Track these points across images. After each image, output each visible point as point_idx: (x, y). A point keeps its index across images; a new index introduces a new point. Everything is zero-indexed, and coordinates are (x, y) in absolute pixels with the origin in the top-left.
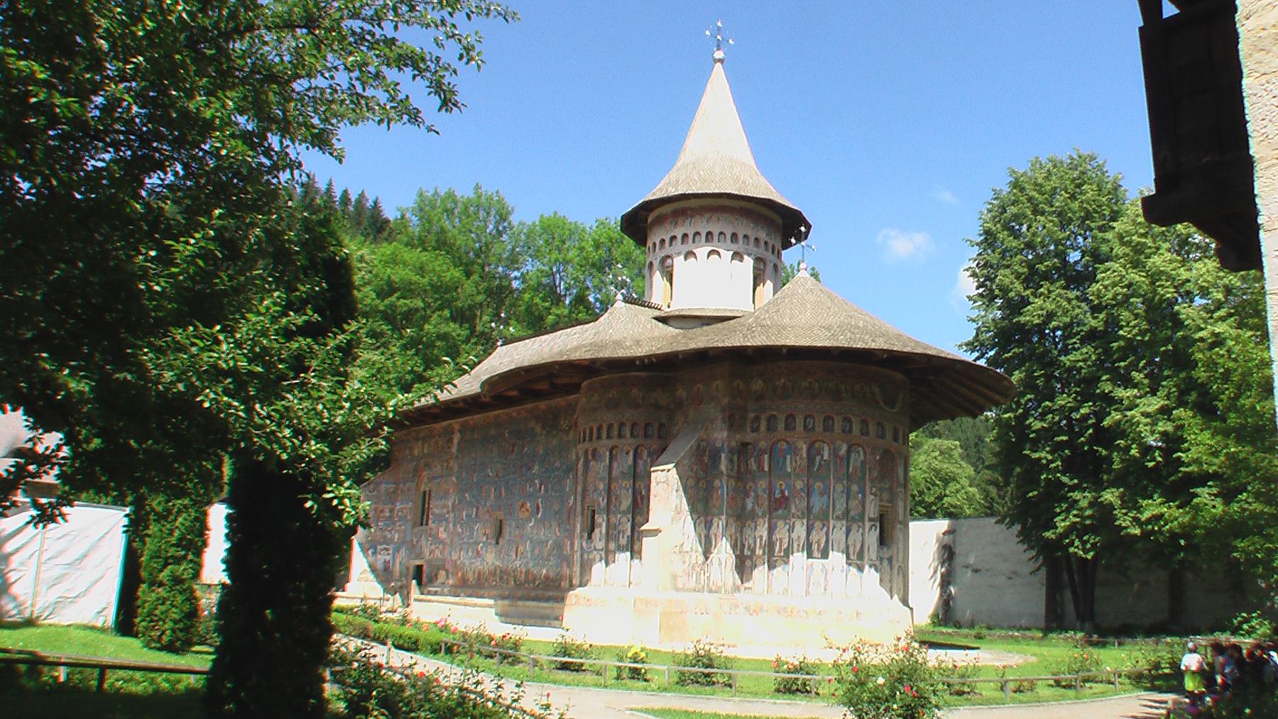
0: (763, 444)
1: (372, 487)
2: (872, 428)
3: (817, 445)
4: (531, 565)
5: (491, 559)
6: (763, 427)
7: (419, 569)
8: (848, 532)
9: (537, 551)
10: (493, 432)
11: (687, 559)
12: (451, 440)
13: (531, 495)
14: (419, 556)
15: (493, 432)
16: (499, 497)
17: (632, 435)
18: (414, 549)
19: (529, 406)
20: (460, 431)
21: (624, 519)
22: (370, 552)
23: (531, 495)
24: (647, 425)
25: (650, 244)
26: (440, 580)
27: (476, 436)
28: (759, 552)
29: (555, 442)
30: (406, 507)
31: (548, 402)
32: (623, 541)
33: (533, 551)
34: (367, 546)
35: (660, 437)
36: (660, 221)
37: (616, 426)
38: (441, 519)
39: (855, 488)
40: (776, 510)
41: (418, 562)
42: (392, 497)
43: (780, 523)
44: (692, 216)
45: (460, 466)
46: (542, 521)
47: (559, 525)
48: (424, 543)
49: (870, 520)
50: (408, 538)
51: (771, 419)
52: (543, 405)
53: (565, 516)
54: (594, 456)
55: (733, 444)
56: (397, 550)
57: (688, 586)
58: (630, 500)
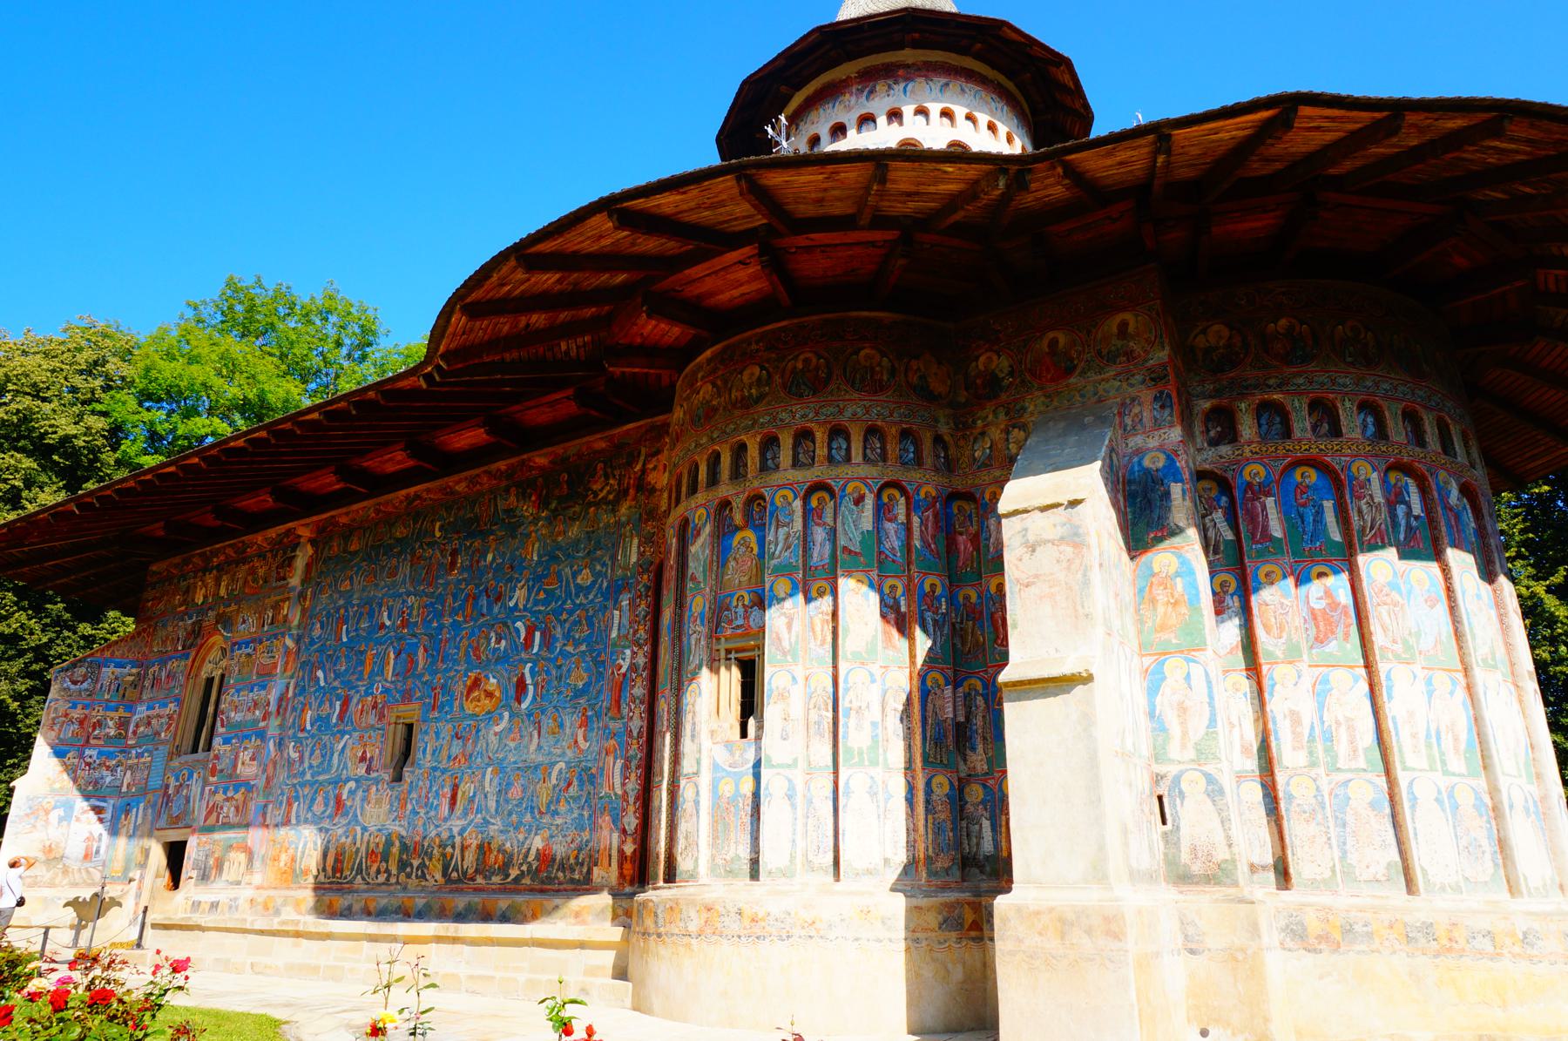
0: (1255, 472)
6: (1247, 429)
9: (515, 792)
10: (400, 532)
13: (502, 659)
15: (400, 532)
19: (502, 465)
20: (312, 542)
23: (502, 659)
24: (905, 434)
27: (352, 548)
29: (574, 531)
30: (158, 713)
31: (559, 449)
33: (502, 792)
40: (1320, 640)
42: (127, 696)
43: (1340, 677)
44: (908, 79)
47: (585, 723)
48: (195, 789)
50: (155, 782)
53: (605, 701)
54: (749, 521)
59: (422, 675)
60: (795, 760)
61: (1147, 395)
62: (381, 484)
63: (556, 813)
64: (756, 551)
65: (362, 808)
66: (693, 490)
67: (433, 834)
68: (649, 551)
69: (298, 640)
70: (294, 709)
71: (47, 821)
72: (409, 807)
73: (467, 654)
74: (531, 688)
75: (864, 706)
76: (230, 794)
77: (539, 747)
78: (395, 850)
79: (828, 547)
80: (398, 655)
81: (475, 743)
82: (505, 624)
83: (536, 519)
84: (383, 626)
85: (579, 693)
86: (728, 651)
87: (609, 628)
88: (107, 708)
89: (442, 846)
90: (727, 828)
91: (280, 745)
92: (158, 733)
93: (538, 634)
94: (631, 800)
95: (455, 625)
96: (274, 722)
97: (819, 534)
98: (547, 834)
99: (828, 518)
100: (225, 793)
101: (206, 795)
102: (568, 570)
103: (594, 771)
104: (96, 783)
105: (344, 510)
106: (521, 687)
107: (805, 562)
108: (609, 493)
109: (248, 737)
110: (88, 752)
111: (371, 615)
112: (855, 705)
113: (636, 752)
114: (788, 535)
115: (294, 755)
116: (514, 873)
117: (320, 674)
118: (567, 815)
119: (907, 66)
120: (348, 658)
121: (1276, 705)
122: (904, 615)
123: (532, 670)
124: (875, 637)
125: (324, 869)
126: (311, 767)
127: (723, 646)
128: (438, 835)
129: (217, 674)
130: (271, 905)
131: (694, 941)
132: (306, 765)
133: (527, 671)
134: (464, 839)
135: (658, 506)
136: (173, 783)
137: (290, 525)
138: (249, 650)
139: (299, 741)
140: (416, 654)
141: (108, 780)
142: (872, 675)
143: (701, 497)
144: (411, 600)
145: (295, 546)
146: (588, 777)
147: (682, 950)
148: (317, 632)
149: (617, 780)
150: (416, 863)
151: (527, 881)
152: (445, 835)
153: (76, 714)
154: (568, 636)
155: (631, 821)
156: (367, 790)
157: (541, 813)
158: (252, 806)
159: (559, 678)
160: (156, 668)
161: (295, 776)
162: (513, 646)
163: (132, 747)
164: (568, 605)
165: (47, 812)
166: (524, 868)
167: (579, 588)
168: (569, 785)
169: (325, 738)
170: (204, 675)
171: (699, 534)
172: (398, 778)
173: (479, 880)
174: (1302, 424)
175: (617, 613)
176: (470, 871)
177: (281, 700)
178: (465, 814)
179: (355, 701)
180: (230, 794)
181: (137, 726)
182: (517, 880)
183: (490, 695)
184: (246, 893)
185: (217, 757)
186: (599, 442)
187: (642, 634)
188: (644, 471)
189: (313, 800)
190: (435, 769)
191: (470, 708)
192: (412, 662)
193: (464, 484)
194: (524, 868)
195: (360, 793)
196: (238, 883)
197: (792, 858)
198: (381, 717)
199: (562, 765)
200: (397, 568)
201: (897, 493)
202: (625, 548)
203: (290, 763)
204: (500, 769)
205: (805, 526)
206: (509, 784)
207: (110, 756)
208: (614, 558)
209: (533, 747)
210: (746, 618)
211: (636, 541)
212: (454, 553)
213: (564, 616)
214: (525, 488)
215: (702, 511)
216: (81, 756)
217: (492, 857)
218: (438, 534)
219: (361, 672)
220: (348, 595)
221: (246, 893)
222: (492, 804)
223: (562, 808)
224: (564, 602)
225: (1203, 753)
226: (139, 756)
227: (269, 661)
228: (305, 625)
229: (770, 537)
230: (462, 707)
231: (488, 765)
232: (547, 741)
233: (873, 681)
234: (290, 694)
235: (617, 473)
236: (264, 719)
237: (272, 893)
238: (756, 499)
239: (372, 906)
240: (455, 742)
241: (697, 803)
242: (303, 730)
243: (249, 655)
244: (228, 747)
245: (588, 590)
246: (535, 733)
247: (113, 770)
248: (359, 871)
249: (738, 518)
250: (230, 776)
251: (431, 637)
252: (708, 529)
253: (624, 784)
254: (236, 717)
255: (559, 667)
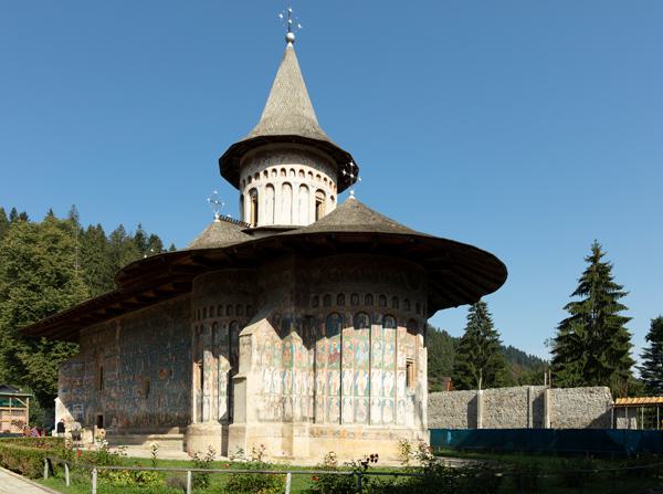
2: (401, 303)
3: (361, 315)
5: (143, 407)
6: (321, 304)
7: (101, 417)
8: (383, 377)
11: (267, 398)
14: (100, 409)
16: (146, 367)
17: (228, 314)
18: (97, 406)
19: (163, 303)
20: (121, 324)
24: (238, 306)
25: (241, 182)
26: (114, 423)
28: (319, 392)
30: (89, 378)
32: (224, 388)
35: (248, 315)
36: (247, 163)
37: (216, 309)
38: (112, 384)
39: (388, 346)
40: (331, 363)
41: (100, 414)
42: (81, 372)
44: (270, 157)
45: (121, 349)
49: (400, 369)
51: (327, 297)
52: (171, 302)
54: (202, 329)
55: (299, 316)
56: (86, 407)
57: (268, 418)
61: (289, 296)
62: (134, 307)
119: (270, 152)
121: (318, 380)
174: (334, 303)
204: (168, 395)
225: (291, 393)
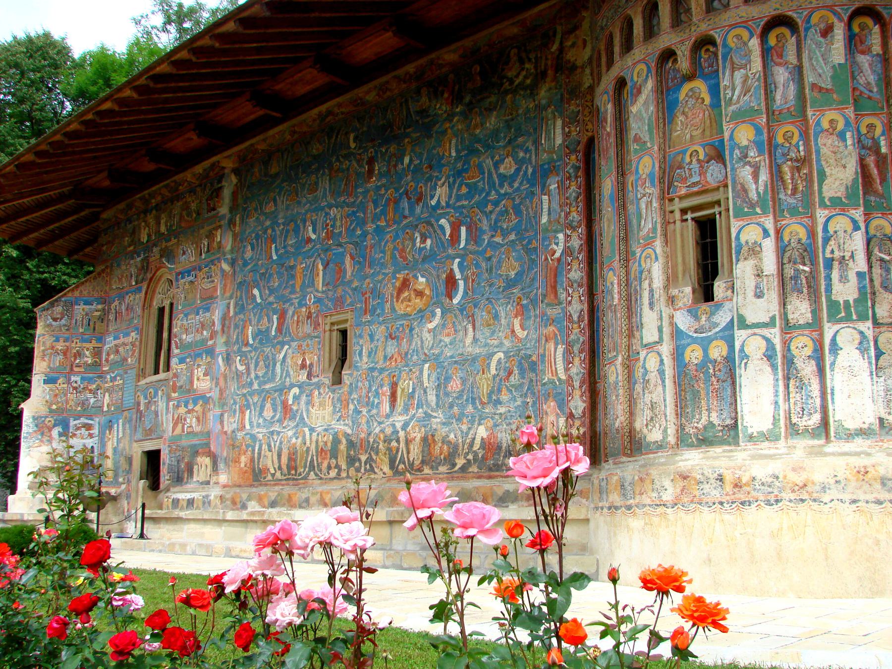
1: (58, 309)
4: (439, 417)
5: (324, 417)
9: (455, 385)
10: (316, 149)
12: (217, 193)
13: (428, 258)
19: (410, 68)
20: (236, 171)
21: (840, 224)
22: (55, 432)
23: (428, 258)
27: (273, 171)
29: (492, 122)
31: (468, 43)
32: (845, 291)
33: (441, 386)
34: (50, 421)
41: (150, 446)
42: (97, 328)
46: (467, 312)
47: (522, 311)
48: (162, 405)
50: (129, 401)
56: (109, 425)
58: (852, 165)
59: (351, 282)
60: (773, 318)
62: (291, 107)
63: (498, 402)
64: (708, 101)
65: (308, 411)
66: (628, 46)
67: (377, 430)
68: (575, 131)
69: (233, 263)
70: (236, 326)
71: (50, 436)
72: (351, 407)
73: (393, 257)
74: (461, 283)
75: (847, 255)
76: (190, 407)
77: (475, 340)
78: (343, 447)
79: (792, 89)
80: (325, 267)
81: (410, 341)
82: (429, 223)
83: (450, 116)
84: (309, 240)
85: (510, 284)
86: (684, 211)
87: (538, 215)
88: (83, 341)
89: (387, 440)
90: (696, 395)
91: (228, 360)
92: (125, 359)
93: (463, 230)
94: (577, 384)
95: (379, 231)
96: (221, 339)
97: (781, 75)
98: (490, 423)
99: (791, 56)
100: (186, 406)
101: (171, 410)
102: (489, 162)
103: (534, 358)
104: (83, 404)
105: (261, 137)
106: (451, 282)
107: (767, 109)
108: (526, 77)
109: (199, 355)
110: (73, 378)
111: (297, 231)
112: (837, 254)
113: (578, 336)
114: (746, 79)
115: (241, 368)
116: (460, 462)
117: (256, 292)
118: (509, 403)
120: (280, 275)
122: (885, 157)
123: (460, 265)
124: (855, 181)
125: (280, 468)
126: (257, 377)
127: (677, 205)
128: (382, 431)
129: (166, 304)
130: (238, 500)
131: (669, 511)
132: (253, 376)
133: (455, 267)
134: (407, 434)
135: (580, 84)
136: (143, 401)
137: (214, 159)
138: (191, 278)
139: (243, 355)
140: (343, 263)
141: (92, 401)
142: (854, 222)
143: (638, 52)
144: (333, 212)
145: (221, 178)
146: (529, 364)
147: (656, 520)
148: (249, 254)
149: (562, 366)
150: (363, 458)
151: (474, 469)
152: (389, 431)
153: (60, 346)
154: (495, 228)
155: (579, 405)
156: (310, 395)
157: (482, 403)
158: (210, 415)
159: (490, 270)
160: (116, 303)
161: (243, 386)
162: (439, 244)
163: (108, 372)
164: (493, 196)
165: (50, 430)
166: (470, 457)
167: (503, 178)
168: (510, 373)
169: (267, 350)
170: (156, 304)
171: (639, 92)
172: (338, 380)
173: (427, 470)
175: (545, 198)
176: (417, 463)
177: (224, 318)
178: (406, 410)
179: (290, 313)
180: (190, 407)
181: (108, 354)
182: (464, 469)
183: (420, 294)
184: (214, 493)
185: (176, 375)
186: (510, 28)
187: (575, 216)
188: (561, 50)
189: (262, 408)
190: (372, 369)
191: (401, 308)
192: (341, 271)
193: (374, 93)
194: (470, 457)
195: (304, 398)
196: (208, 483)
197: (775, 420)
198: (317, 325)
199: (501, 355)
200: (316, 183)
201: (869, 21)
202: (548, 132)
203: (239, 375)
205: (765, 66)
206: (448, 379)
207: (90, 381)
208: (537, 143)
209: (469, 340)
210: (702, 173)
211: (559, 123)
212: (371, 162)
213: (490, 208)
214: (436, 87)
215: (642, 67)
216: (69, 382)
217: (437, 448)
218: (353, 145)
219: (293, 286)
220: (273, 216)
221: (214, 493)
222: (432, 398)
223: (505, 397)
224: (488, 194)
226: (113, 379)
227: (209, 286)
228: (237, 249)
229: (725, 82)
230: (393, 309)
231: (425, 361)
232: (483, 334)
233: (856, 228)
234: (232, 313)
235: (532, 56)
236: (211, 338)
237: (238, 490)
238: (705, 42)
239: (327, 499)
240: (390, 342)
241: (661, 373)
242: (247, 344)
243: (192, 282)
244: (183, 366)
245: (512, 179)
246: (470, 329)
247: (94, 393)
248: (312, 467)
249: (684, 64)
250: (189, 391)
251: (356, 244)
252: (650, 84)
253: (567, 370)
254: (187, 338)
255: (489, 259)
